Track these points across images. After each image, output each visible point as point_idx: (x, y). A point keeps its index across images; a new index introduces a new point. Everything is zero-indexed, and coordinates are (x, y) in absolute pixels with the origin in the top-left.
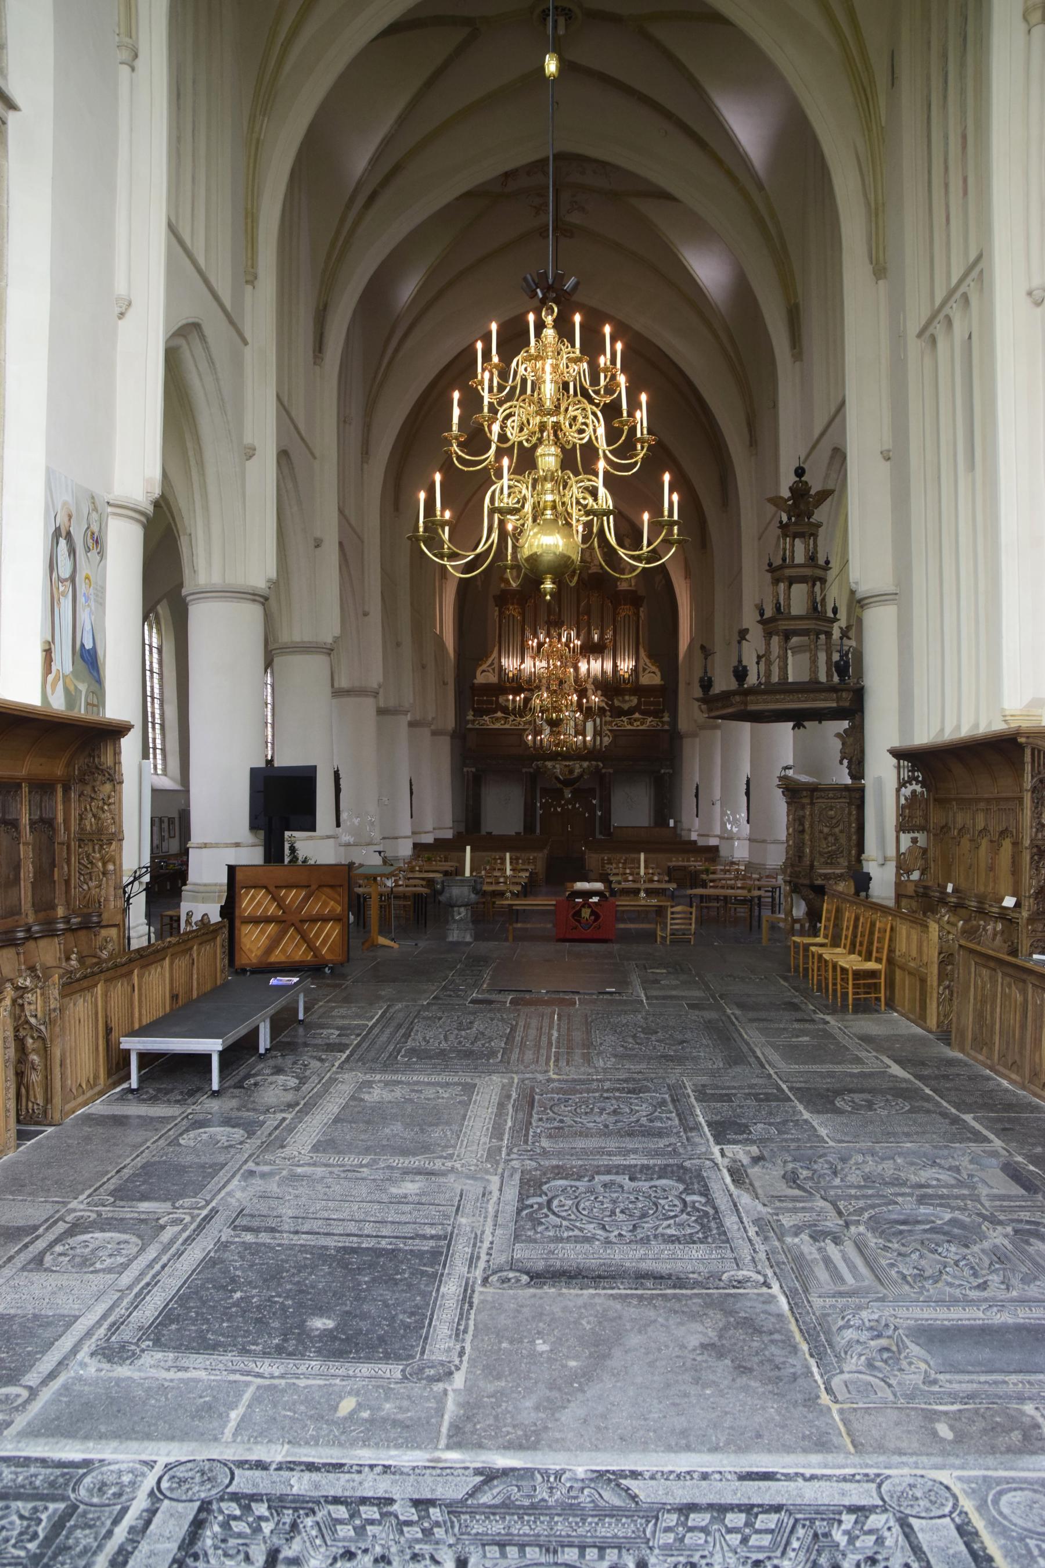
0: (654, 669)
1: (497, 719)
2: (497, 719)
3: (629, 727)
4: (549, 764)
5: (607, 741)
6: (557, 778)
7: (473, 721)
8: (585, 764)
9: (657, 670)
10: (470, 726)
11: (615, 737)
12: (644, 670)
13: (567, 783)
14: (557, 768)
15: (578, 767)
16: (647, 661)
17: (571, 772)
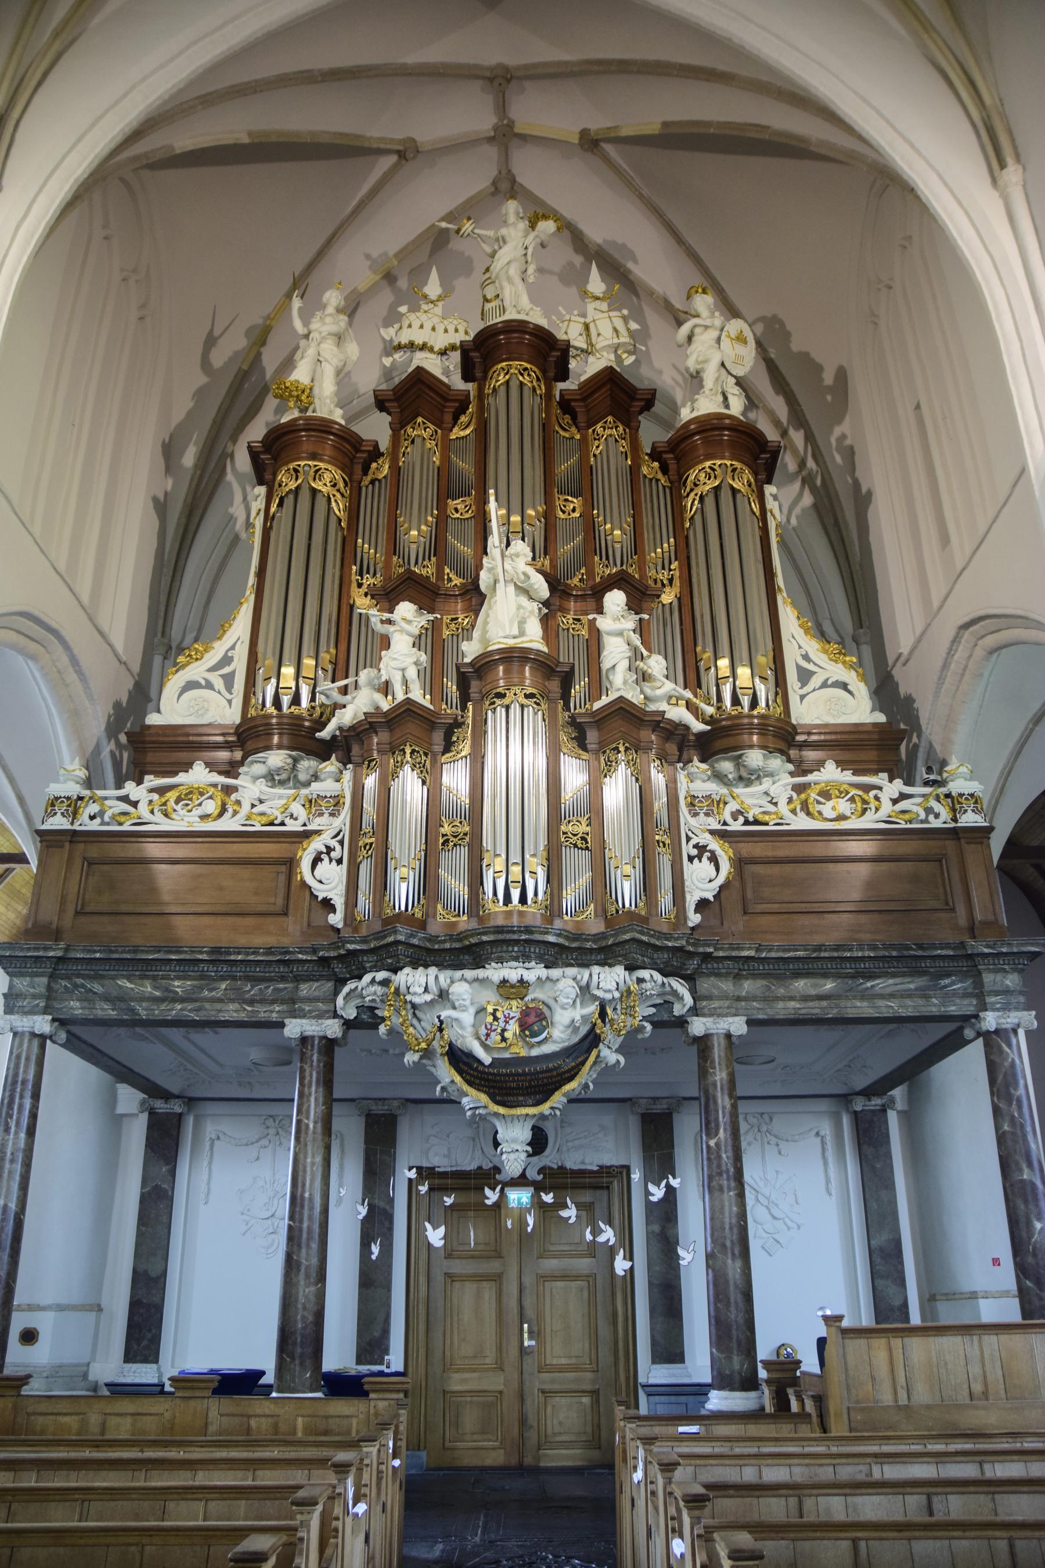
0: (838, 672)
1: (187, 796)
2: (187, 796)
3: (802, 823)
4: (416, 981)
5: (703, 880)
6: (459, 1058)
7: (73, 806)
8: (610, 979)
9: (851, 677)
10: (59, 822)
11: (740, 863)
12: (805, 676)
13: (514, 1083)
14: (466, 1007)
15: (568, 1000)
16: (812, 646)
17: (534, 1021)
